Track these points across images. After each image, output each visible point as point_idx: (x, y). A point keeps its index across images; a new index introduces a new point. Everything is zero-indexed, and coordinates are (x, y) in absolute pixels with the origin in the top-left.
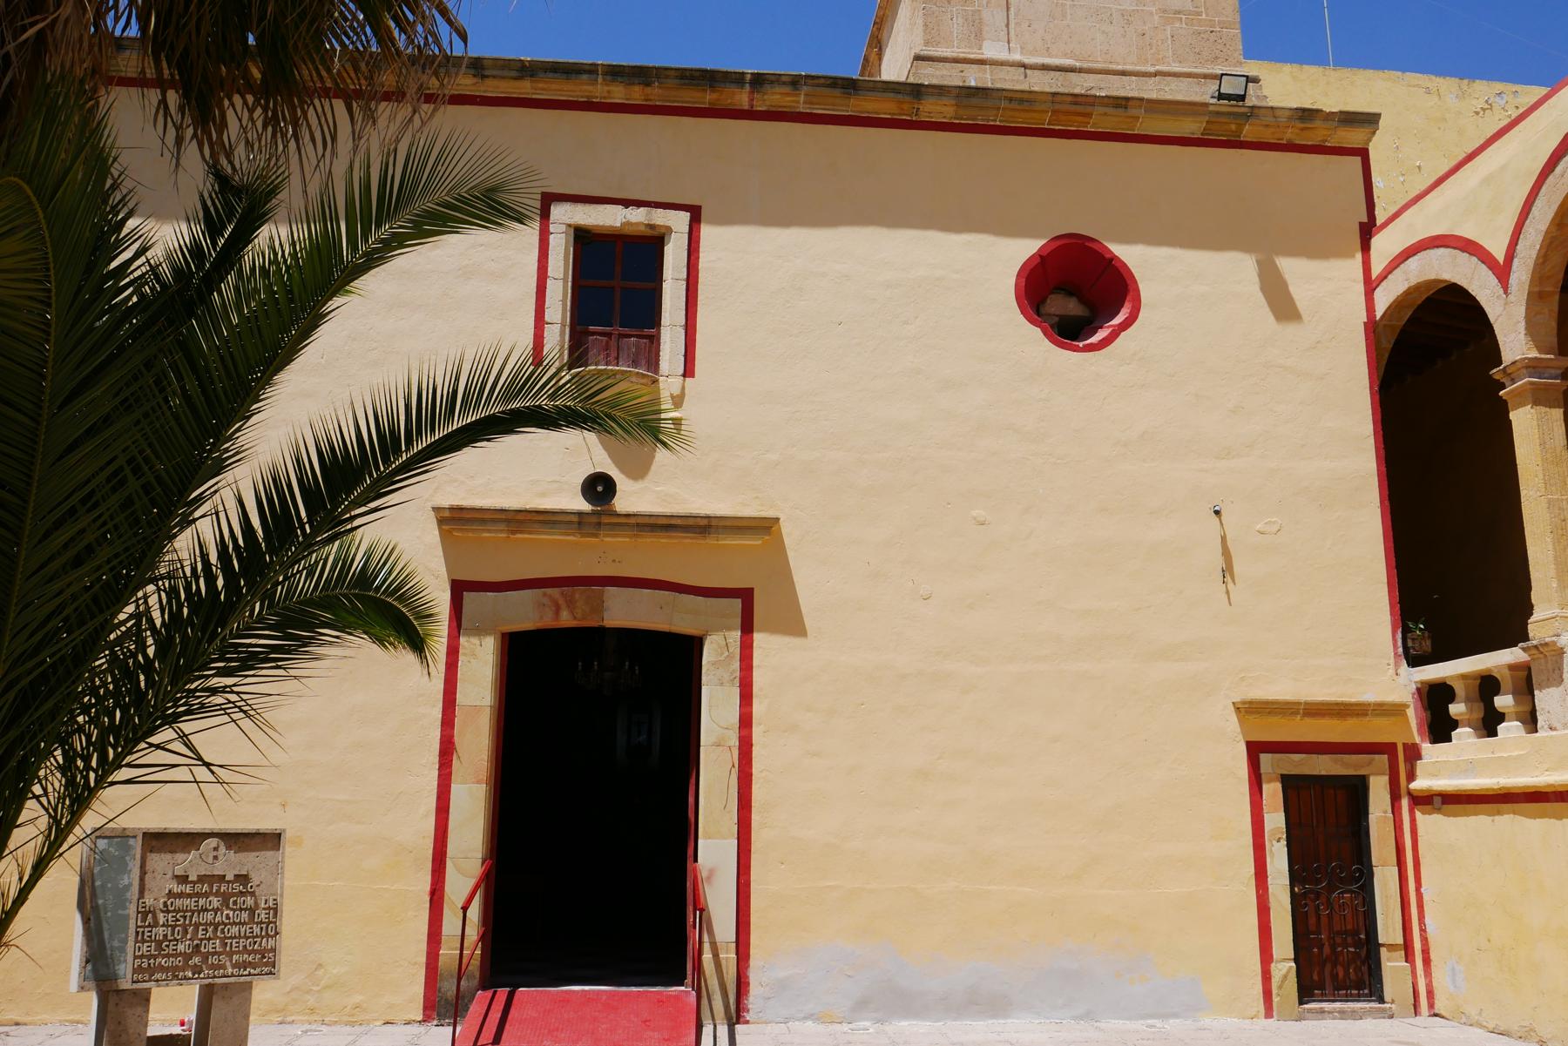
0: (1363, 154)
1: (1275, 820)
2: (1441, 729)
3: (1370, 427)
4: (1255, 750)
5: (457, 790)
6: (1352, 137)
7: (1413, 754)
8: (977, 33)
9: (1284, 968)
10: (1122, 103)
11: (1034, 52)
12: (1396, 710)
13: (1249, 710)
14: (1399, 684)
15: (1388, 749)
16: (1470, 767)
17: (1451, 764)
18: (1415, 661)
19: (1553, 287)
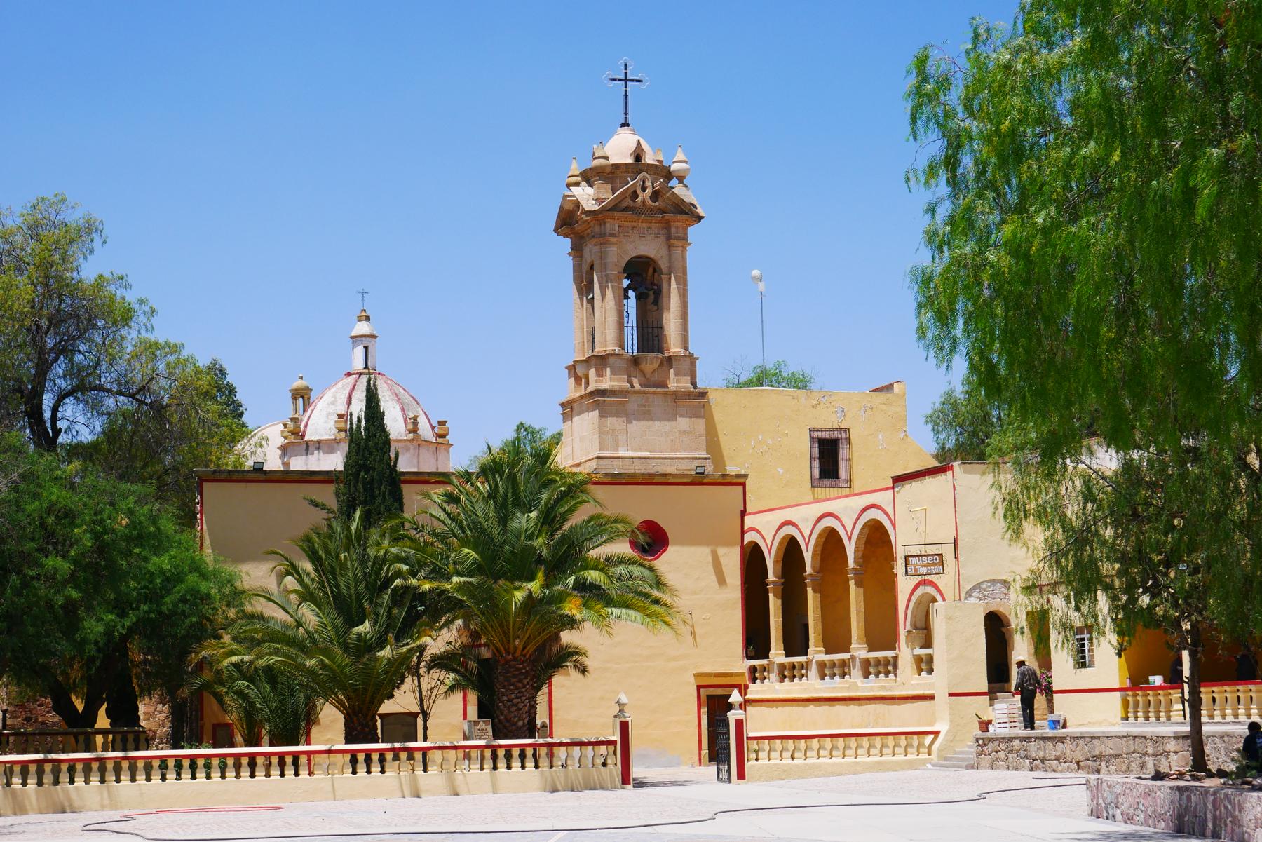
0: (744, 485)
1: (704, 710)
2: (754, 680)
3: (739, 582)
4: (699, 688)
5: (469, 708)
6: (741, 480)
7: (746, 687)
8: (617, 447)
9: (705, 752)
10: (664, 475)
11: (636, 450)
12: (742, 674)
13: (697, 676)
14: (741, 665)
15: (738, 686)
16: (757, 692)
17: (756, 691)
18: (749, 658)
19: (781, 559)
